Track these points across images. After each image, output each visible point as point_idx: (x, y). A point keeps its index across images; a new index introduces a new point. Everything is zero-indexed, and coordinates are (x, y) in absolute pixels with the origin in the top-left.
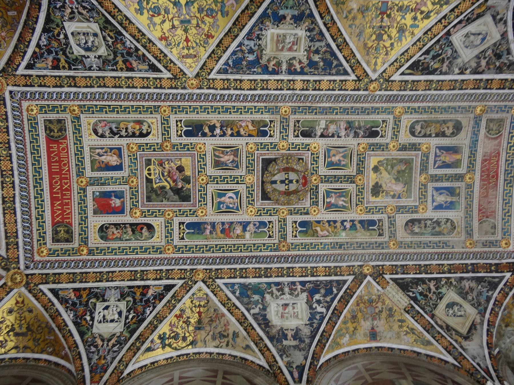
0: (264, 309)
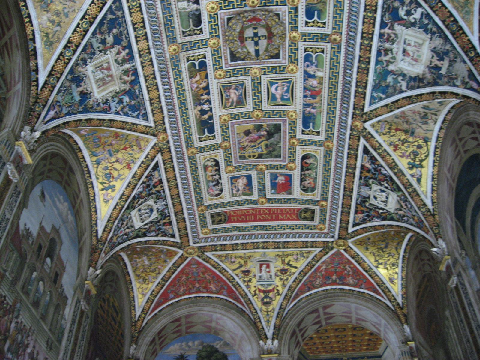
0: (404, 76)
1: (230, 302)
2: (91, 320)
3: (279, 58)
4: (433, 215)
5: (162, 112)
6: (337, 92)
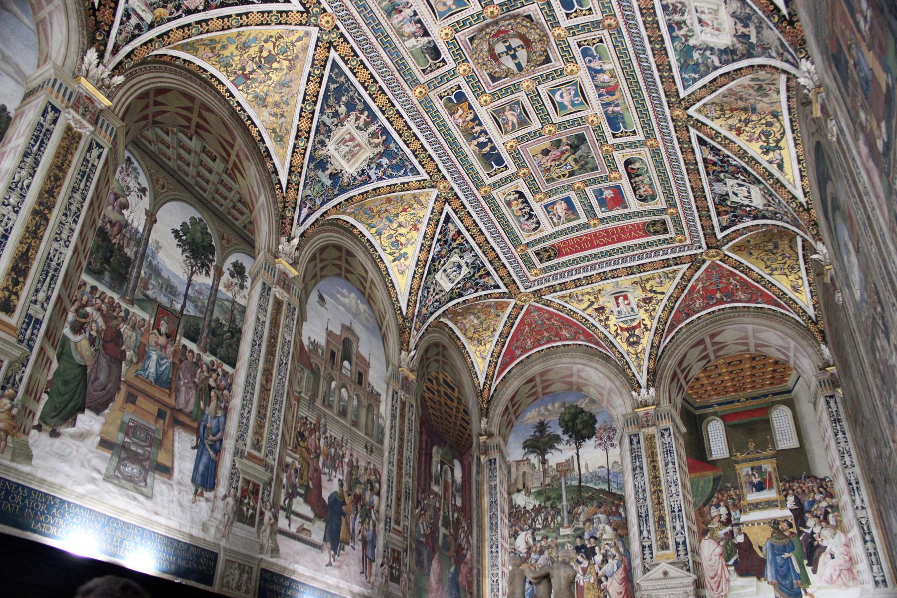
0: (712, 49)
2: (417, 407)
3: (551, 62)
4: (808, 210)
5: (432, 160)
6: (638, 82)
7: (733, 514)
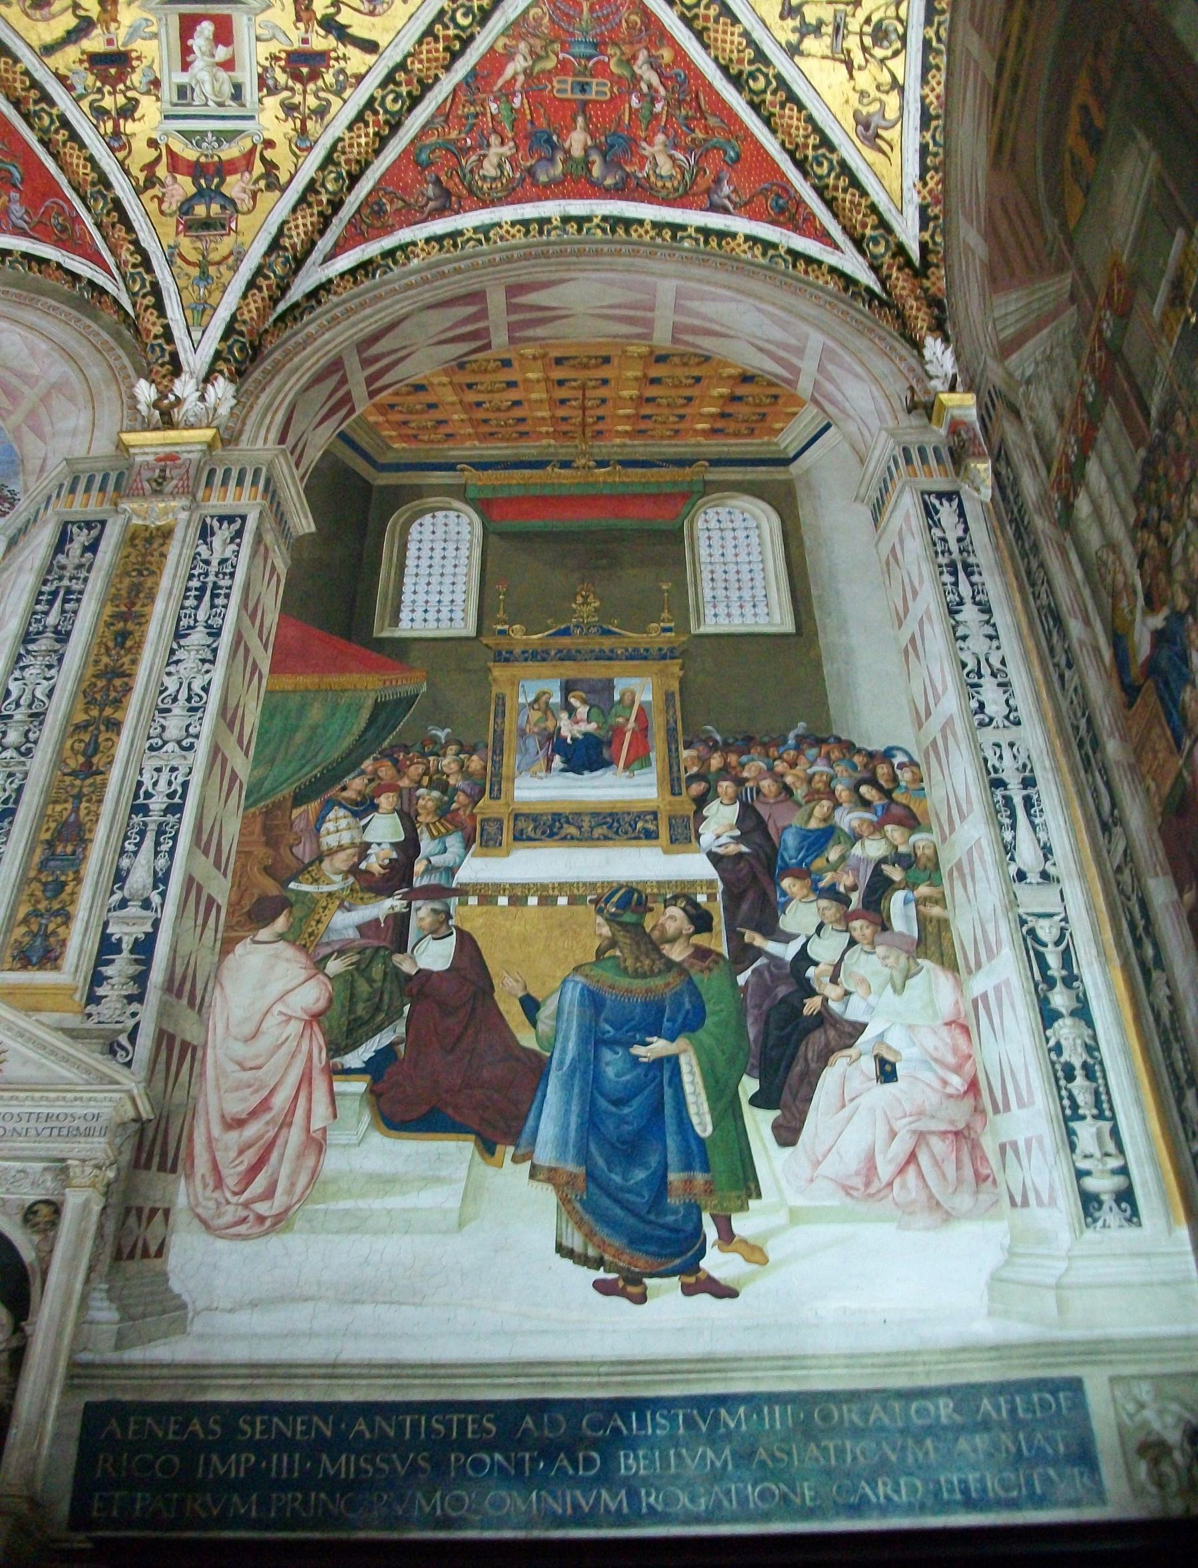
1: (43, 262)
7: (427, 845)
